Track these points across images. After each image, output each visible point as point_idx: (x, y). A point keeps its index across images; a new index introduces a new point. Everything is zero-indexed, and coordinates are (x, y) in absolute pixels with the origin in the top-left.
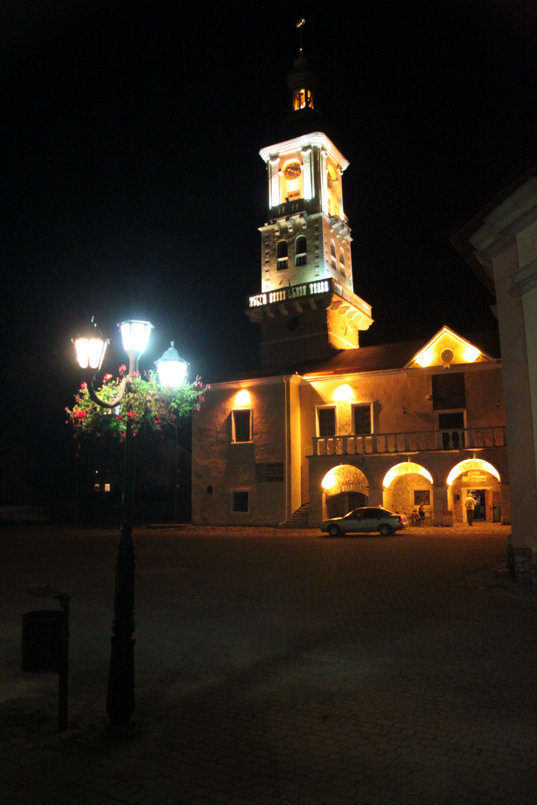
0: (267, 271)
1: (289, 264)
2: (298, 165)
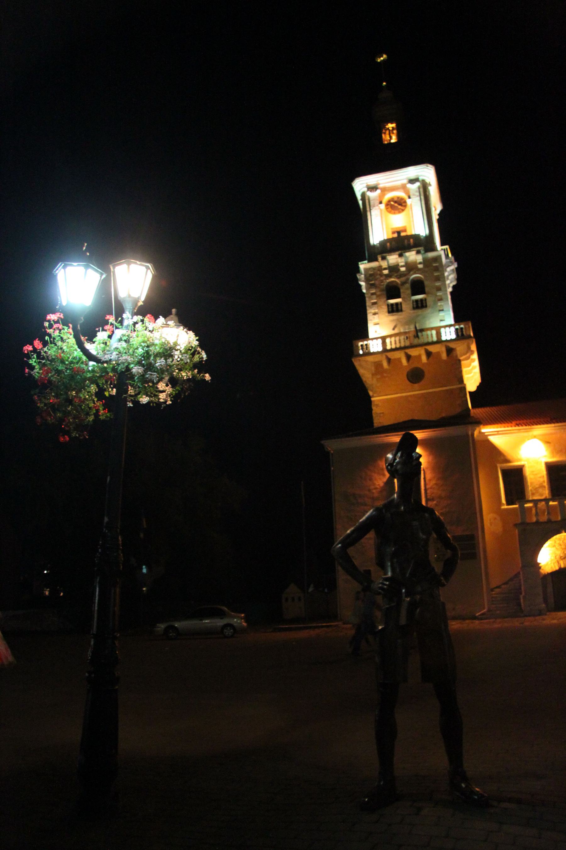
0: (375, 314)
1: (404, 306)
2: (402, 199)
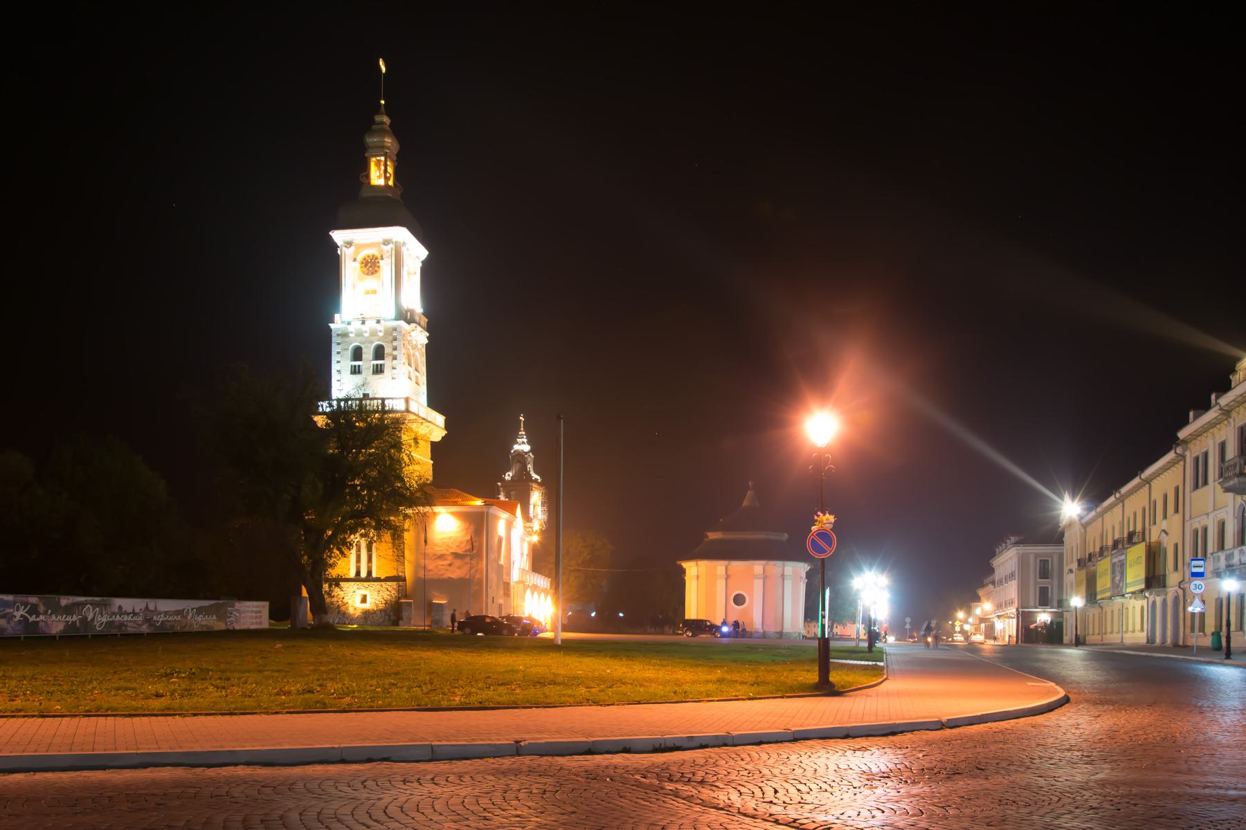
1: (363, 368)
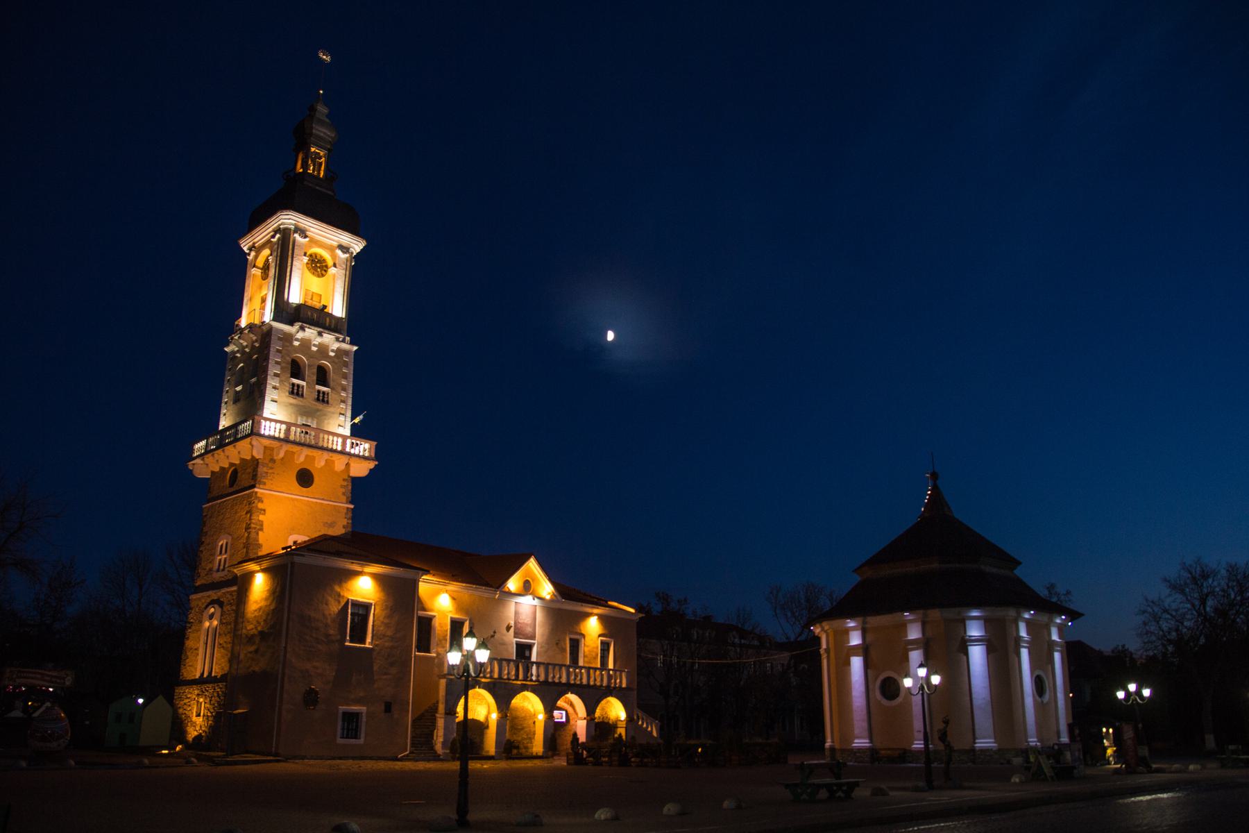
0: (275, 388)
